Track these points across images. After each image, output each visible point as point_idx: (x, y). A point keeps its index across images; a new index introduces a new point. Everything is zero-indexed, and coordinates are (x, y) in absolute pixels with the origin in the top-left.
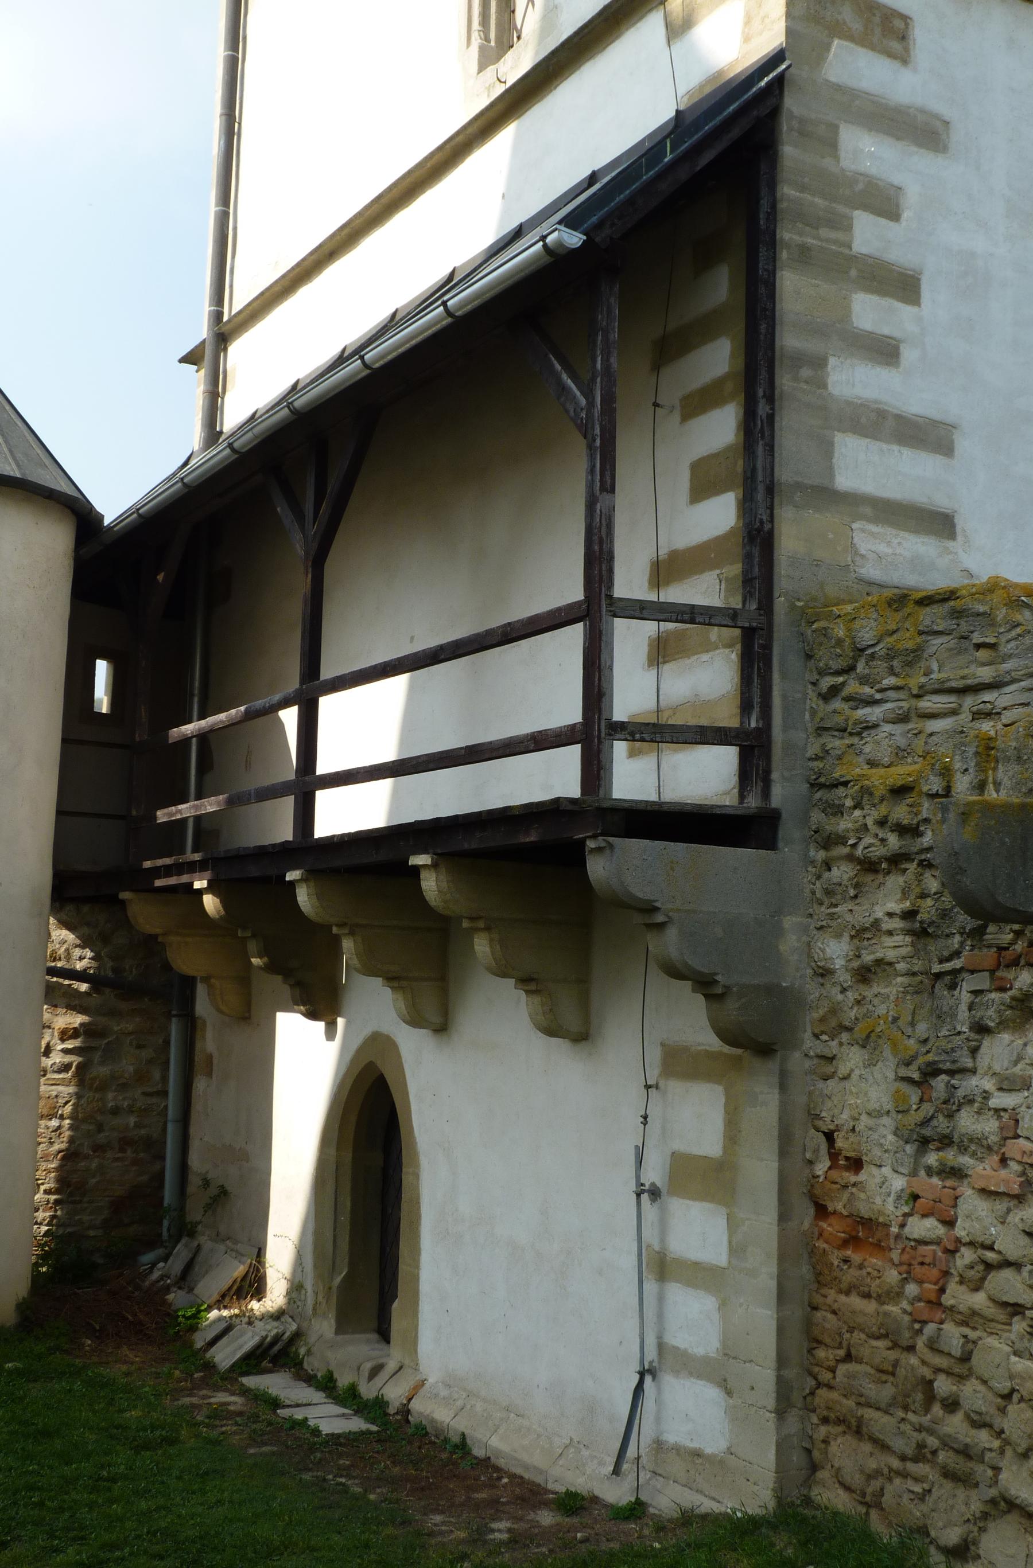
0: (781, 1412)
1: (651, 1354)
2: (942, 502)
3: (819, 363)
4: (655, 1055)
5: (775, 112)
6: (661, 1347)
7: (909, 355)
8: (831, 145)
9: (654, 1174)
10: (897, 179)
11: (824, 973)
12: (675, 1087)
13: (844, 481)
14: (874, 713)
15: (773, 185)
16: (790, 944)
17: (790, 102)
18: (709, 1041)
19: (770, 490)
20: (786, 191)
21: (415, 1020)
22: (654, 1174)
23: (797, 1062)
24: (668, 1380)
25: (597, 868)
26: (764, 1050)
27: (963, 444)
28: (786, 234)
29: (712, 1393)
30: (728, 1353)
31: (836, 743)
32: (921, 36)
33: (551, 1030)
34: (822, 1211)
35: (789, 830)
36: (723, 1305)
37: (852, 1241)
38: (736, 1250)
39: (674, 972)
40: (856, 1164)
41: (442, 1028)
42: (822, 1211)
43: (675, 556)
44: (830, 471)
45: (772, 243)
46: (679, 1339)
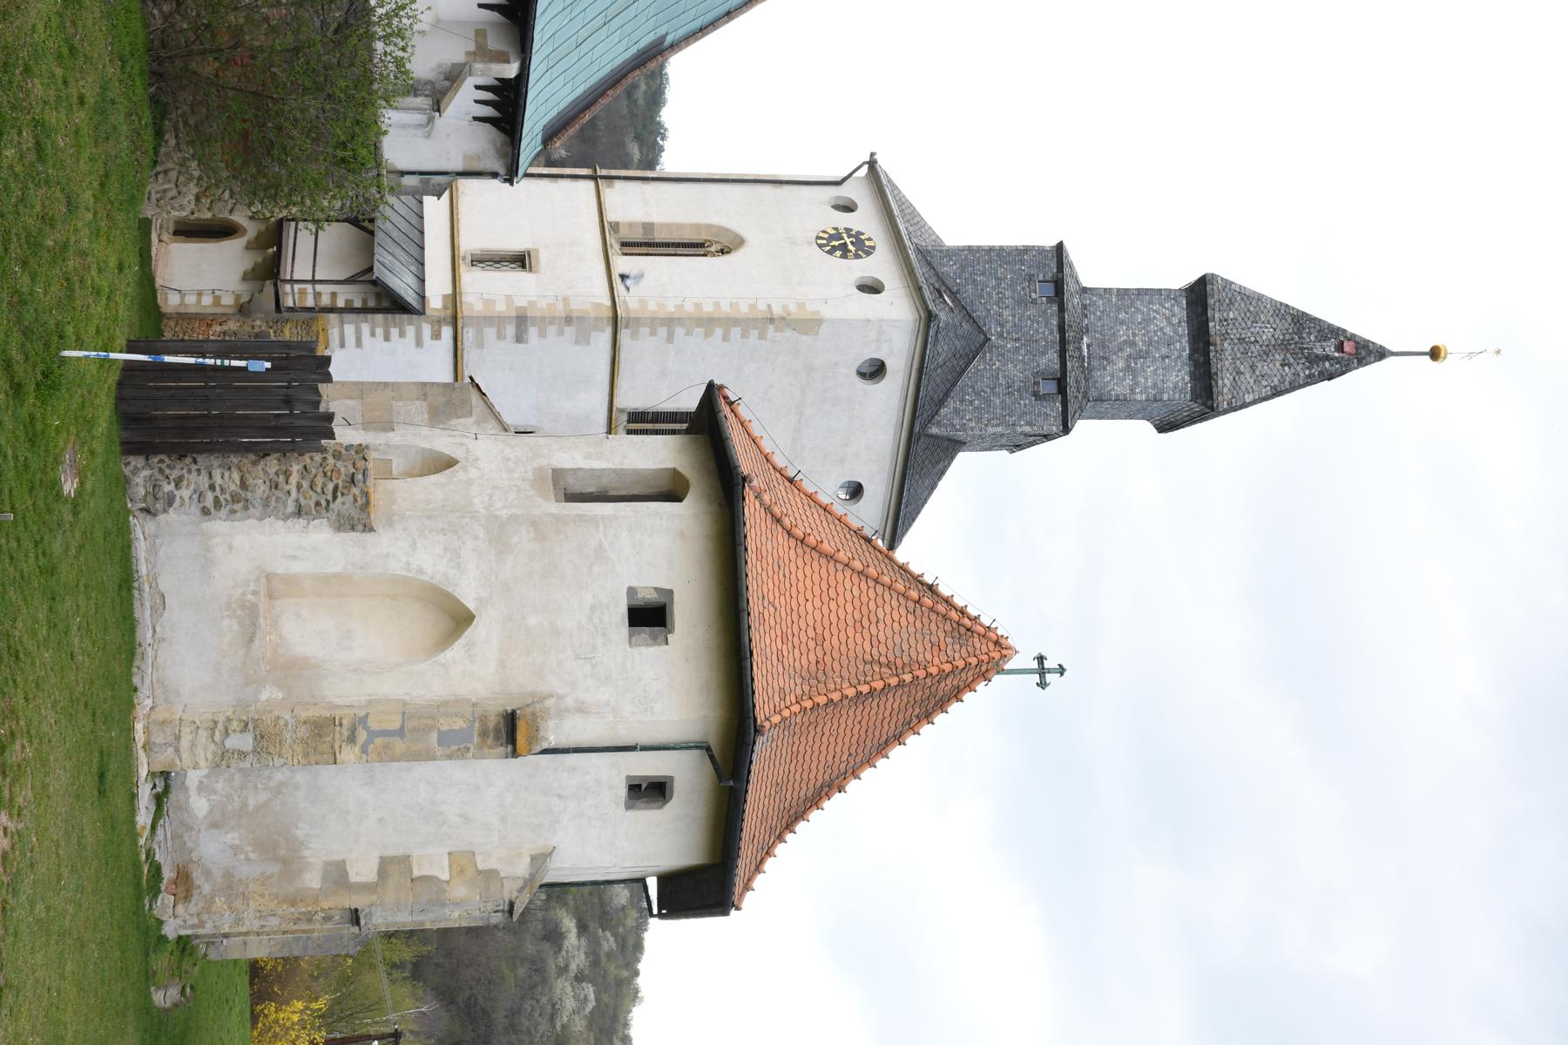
0: (177, 313)
1: (184, 292)
2: (346, 346)
3: (367, 322)
4: (240, 293)
5: (412, 314)
6: (185, 294)
7: (373, 339)
8: (410, 324)
9: (217, 293)
10: (408, 336)
11: (254, 321)
12: (234, 296)
13: (346, 326)
14: (299, 328)
15: (399, 313)
16: (259, 315)
17: (415, 317)
18: (242, 301)
19: (341, 312)
20: (398, 316)
21: (248, 242)
22: (217, 293)
23: (238, 316)
24: (179, 295)
25: (268, 282)
26: (240, 311)
27: (358, 350)
28: (389, 316)
29: (178, 302)
30: (186, 305)
31: (295, 323)
32: (438, 342)
33: (245, 273)
34: (212, 321)
35: (279, 315)
36: (194, 305)
37: (207, 324)
38: (205, 306)
39: (252, 295)
40: (220, 325)
41: (248, 247)
42: (212, 321)
43: (336, 296)
44: (346, 323)
45: (388, 313)
46: (186, 297)
